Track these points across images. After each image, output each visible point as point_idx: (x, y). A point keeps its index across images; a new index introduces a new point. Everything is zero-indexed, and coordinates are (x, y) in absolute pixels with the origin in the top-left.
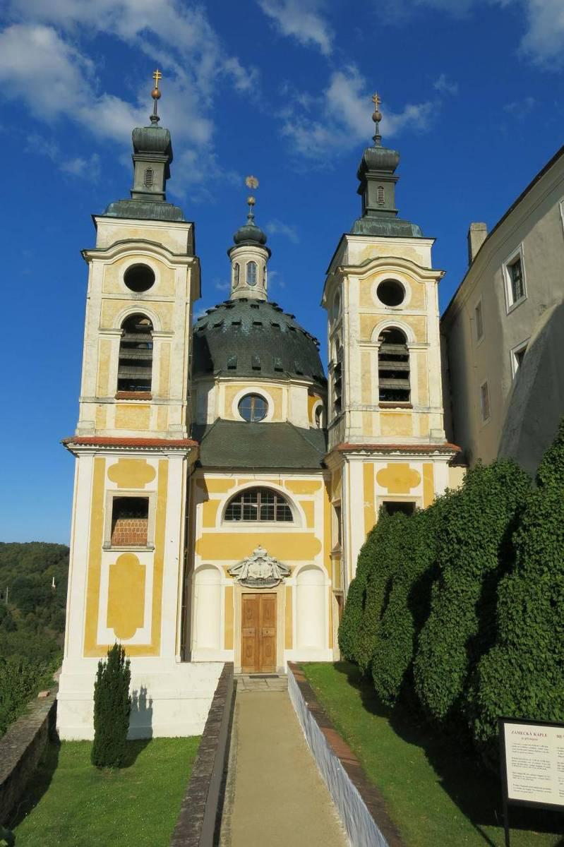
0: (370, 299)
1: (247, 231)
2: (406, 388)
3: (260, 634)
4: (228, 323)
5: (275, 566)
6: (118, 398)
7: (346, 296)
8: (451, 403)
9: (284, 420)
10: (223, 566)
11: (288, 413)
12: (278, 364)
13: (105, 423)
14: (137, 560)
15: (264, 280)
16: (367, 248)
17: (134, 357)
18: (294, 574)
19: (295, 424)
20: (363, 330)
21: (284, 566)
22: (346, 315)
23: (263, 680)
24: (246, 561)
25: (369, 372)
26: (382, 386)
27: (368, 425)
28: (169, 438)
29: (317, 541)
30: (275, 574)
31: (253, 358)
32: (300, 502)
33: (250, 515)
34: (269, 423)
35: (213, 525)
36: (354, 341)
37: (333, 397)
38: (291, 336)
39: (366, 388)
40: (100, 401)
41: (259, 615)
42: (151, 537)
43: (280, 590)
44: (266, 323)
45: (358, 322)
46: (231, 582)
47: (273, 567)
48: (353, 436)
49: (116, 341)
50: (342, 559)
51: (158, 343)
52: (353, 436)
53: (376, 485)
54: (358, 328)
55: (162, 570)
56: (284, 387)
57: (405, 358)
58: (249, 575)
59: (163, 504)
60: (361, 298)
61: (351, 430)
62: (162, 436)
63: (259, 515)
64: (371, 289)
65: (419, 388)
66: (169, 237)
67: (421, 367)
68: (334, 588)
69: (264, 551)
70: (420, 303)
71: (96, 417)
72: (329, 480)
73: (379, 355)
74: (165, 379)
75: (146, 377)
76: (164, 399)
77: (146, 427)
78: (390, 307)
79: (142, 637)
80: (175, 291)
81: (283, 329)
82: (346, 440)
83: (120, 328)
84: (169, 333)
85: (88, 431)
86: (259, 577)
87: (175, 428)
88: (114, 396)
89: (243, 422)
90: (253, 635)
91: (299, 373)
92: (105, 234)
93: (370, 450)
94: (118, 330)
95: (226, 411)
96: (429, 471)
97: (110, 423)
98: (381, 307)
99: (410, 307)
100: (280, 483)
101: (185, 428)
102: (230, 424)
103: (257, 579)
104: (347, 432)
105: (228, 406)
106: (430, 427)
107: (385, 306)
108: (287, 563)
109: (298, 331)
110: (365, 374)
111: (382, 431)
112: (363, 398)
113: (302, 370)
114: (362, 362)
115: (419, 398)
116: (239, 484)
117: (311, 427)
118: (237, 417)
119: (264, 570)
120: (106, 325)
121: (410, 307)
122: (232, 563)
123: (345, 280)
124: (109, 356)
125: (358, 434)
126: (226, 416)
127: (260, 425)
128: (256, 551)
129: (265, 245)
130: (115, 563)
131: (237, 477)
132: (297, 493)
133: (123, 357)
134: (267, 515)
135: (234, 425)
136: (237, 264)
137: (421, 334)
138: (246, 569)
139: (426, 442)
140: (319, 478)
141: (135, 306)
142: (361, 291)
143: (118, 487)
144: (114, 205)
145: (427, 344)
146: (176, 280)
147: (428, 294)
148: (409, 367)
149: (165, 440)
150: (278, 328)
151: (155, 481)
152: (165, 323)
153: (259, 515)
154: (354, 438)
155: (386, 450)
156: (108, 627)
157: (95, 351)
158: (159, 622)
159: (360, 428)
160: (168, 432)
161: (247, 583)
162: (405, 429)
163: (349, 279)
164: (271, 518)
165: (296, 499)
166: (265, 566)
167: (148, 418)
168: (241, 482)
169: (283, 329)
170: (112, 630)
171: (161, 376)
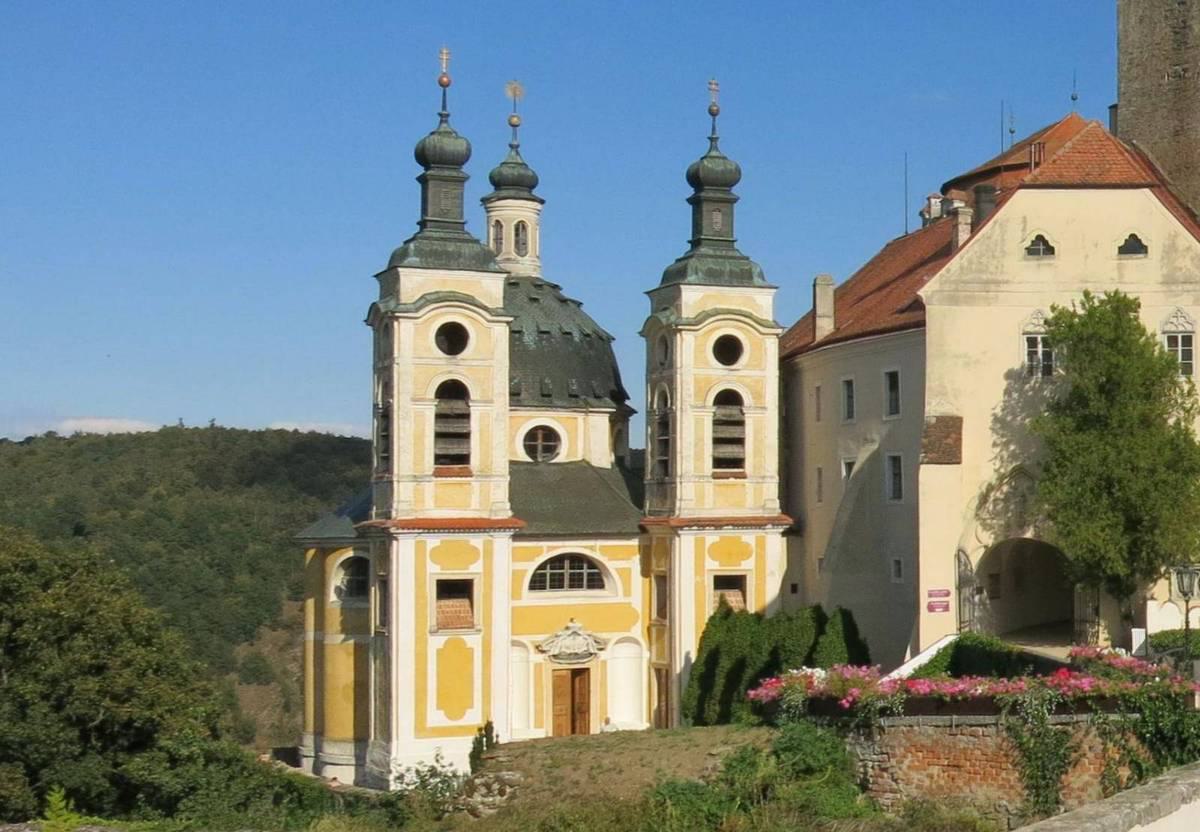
1: (513, 174)
2: (741, 456)
5: (590, 640)
9: (580, 459)
10: (532, 642)
11: (584, 449)
18: (610, 647)
19: (595, 463)
22: (678, 376)
25: (703, 440)
26: (716, 455)
27: (700, 497)
29: (635, 611)
31: (541, 382)
32: (617, 569)
33: (557, 583)
35: (520, 598)
36: (686, 406)
38: (586, 346)
39: (699, 457)
44: (555, 331)
45: (692, 389)
46: (540, 658)
48: (684, 509)
52: (684, 509)
56: (580, 417)
57: (741, 423)
58: (563, 650)
60: (696, 357)
61: (683, 503)
63: (566, 582)
68: (654, 660)
70: (758, 364)
72: (648, 543)
81: (577, 337)
82: (677, 512)
86: (572, 651)
89: (528, 463)
91: (597, 397)
93: (701, 524)
100: (592, 548)
103: (570, 654)
104: (678, 504)
107: (720, 365)
108: (603, 636)
109: (594, 336)
110: (699, 440)
111: (714, 503)
112: (695, 468)
116: (548, 551)
119: (578, 645)
121: (746, 367)
123: (678, 335)
125: (689, 507)
127: (553, 468)
128: (570, 625)
129: (536, 192)
131: (545, 544)
134: (576, 583)
135: (522, 468)
136: (498, 221)
137: (758, 396)
139: (759, 513)
140: (635, 542)
145: (764, 408)
148: (744, 432)
150: (569, 336)
153: (566, 582)
154: (686, 511)
155: (717, 524)
159: (691, 500)
163: (684, 336)
164: (581, 586)
165: (611, 565)
169: (577, 337)
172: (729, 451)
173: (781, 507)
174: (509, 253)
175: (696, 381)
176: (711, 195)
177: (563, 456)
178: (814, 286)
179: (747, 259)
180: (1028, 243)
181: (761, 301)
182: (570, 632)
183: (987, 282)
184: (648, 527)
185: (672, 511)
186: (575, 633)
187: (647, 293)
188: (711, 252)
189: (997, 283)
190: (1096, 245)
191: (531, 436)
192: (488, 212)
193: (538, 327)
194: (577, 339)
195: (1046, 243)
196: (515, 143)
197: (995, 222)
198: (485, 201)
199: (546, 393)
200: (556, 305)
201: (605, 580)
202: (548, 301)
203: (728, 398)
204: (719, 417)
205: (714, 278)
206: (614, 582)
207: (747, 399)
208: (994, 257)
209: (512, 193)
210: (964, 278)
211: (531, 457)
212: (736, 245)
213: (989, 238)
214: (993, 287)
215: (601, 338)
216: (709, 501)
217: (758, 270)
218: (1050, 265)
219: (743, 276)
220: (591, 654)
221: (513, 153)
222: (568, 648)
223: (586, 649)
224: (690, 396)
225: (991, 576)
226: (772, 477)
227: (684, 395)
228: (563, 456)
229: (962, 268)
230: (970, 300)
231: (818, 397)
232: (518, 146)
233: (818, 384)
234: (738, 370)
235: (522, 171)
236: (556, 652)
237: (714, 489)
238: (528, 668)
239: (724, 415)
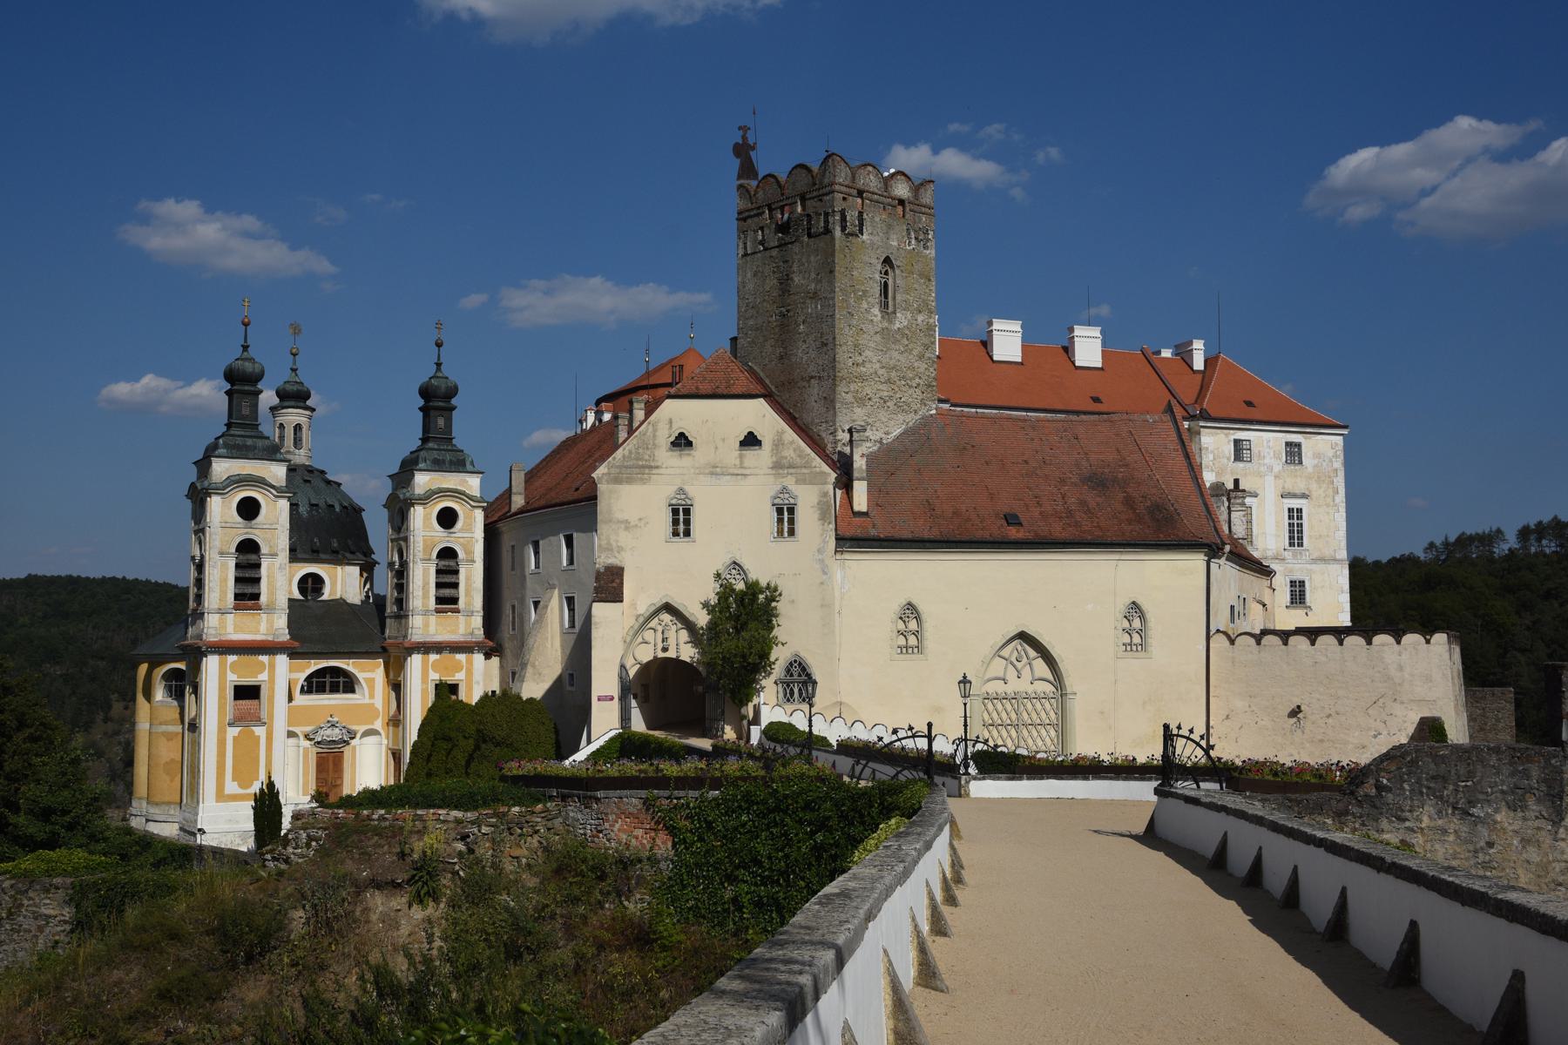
0: (431, 524)
7: (412, 521)
9: (338, 596)
14: (253, 732)
17: (247, 575)
18: (358, 736)
24: (321, 728)
25: (428, 584)
27: (426, 625)
31: (312, 541)
33: (321, 689)
37: (392, 595)
39: (425, 596)
40: (222, 612)
42: (264, 715)
43: (347, 750)
44: (322, 504)
45: (421, 544)
47: (344, 731)
49: (232, 563)
50: (401, 727)
51: (265, 564)
54: (421, 549)
56: (339, 568)
57: (456, 572)
58: (324, 738)
59: (272, 690)
60: (424, 523)
61: (414, 630)
62: (270, 638)
63: (328, 688)
65: (466, 596)
66: (271, 472)
67: (468, 578)
68: (390, 746)
69: (336, 719)
70: (469, 528)
74: (272, 592)
75: (256, 591)
76: (271, 609)
77: (257, 632)
81: (338, 509)
83: (234, 551)
84: (274, 555)
85: (215, 636)
87: (281, 631)
92: (219, 469)
96: (470, 663)
97: (230, 629)
101: (287, 631)
104: (410, 630)
106: (473, 626)
107: (442, 530)
108: (354, 727)
110: (426, 584)
112: (423, 603)
114: (423, 576)
115: (465, 604)
119: (335, 734)
120: (225, 549)
121: (461, 531)
122: (308, 729)
128: (330, 719)
129: (309, 403)
130: (236, 735)
133: (238, 575)
134: (335, 689)
136: (281, 425)
137: (469, 552)
141: (247, 533)
145: (474, 562)
146: (278, 510)
147: (477, 520)
149: (273, 641)
152: (271, 547)
153: (328, 688)
165: (360, 676)
167: (259, 623)
168: (315, 664)
169: (338, 509)
172: (447, 592)
173: (484, 634)
174: (289, 447)
175: (424, 540)
176: (436, 404)
177: (325, 597)
178: (511, 471)
179: (462, 451)
180: (672, 439)
181: (472, 484)
183: (643, 467)
184: (388, 648)
185: (405, 636)
186: (333, 725)
187: (389, 476)
188: (436, 447)
189: (651, 467)
190: (724, 440)
191: (303, 581)
192: (274, 417)
193: (309, 501)
194: (337, 510)
195: (686, 438)
196: (294, 367)
197: (649, 423)
198: (273, 409)
199: (315, 548)
200: (323, 485)
201: (356, 687)
202: (317, 482)
203: (448, 553)
204: (440, 567)
205: (438, 466)
206: (363, 688)
207: (461, 555)
208: (647, 448)
209: (292, 403)
210: (626, 464)
212: (454, 441)
213: (644, 434)
214: (647, 471)
215: (355, 509)
216: (432, 629)
217: (470, 459)
218: (689, 455)
219: (459, 464)
220: (345, 741)
221: (293, 374)
222: (328, 737)
225: (642, 685)
226: (478, 612)
227: (416, 551)
228: (325, 597)
229: (624, 456)
230: (630, 481)
231: (513, 552)
232: (297, 370)
233: (513, 543)
235: (300, 388)
236: (320, 739)
238: (299, 751)
239: (444, 566)
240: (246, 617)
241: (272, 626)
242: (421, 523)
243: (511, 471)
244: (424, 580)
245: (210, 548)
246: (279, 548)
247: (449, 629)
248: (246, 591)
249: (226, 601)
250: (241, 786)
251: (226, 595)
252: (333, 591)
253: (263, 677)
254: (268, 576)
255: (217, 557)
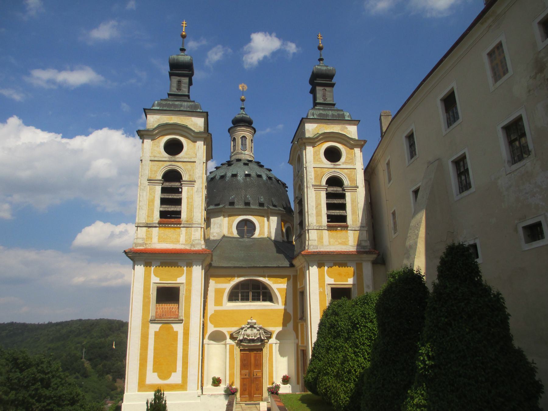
0: (320, 158)
3: (252, 375)
4: (229, 174)
6: (159, 223)
8: (373, 224)
10: (227, 331)
12: (261, 200)
13: (152, 239)
14: (172, 328)
15: (252, 147)
16: (317, 127)
17: (170, 197)
18: (274, 336)
20: (315, 178)
21: (267, 330)
23: (254, 406)
25: (320, 204)
26: (329, 213)
27: (320, 238)
28: (193, 249)
30: (262, 336)
32: (278, 289)
33: (245, 298)
34: (257, 238)
35: (221, 305)
36: (310, 185)
39: (319, 214)
41: (251, 363)
44: (253, 174)
45: (313, 174)
53: (326, 277)
55: (188, 334)
58: (245, 337)
59: (189, 291)
60: (314, 158)
62: (188, 247)
64: (320, 152)
66: (192, 121)
69: (254, 321)
71: (146, 236)
73: (327, 194)
74: (190, 210)
75: (178, 209)
78: (333, 163)
79: (176, 378)
80: (196, 155)
81: (264, 178)
82: (307, 248)
83: (160, 178)
85: (141, 245)
86: (251, 338)
87: (197, 242)
88: (157, 222)
89: (238, 238)
90: (247, 376)
94: (160, 181)
95: (228, 231)
97: (155, 239)
98: (327, 163)
99: (345, 163)
102: (230, 239)
105: (230, 227)
107: (329, 163)
108: (270, 329)
109: (274, 179)
110: (318, 205)
111: (329, 242)
112: (317, 221)
113: (277, 204)
114: (316, 198)
117: (283, 240)
118: (235, 233)
121: (343, 163)
122: (234, 329)
124: (154, 197)
126: (228, 233)
128: (249, 321)
132: (275, 283)
133: (163, 197)
134: (256, 298)
135: (234, 240)
137: (353, 180)
138: (243, 333)
142: (314, 153)
143: (160, 281)
144: (158, 102)
151: (184, 276)
152: (190, 175)
156: (153, 372)
157: (145, 194)
158: (187, 368)
159: (315, 240)
160: (192, 245)
161: (244, 342)
162: (344, 240)
166: (255, 331)
167: (180, 236)
169: (264, 178)
170: (156, 374)
171: (187, 208)
174: (238, 150)
182: (249, 326)
199: (247, 201)
203: (335, 181)
207: (346, 182)
211: (239, 235)
222: (248, 336)
223: (259, 336)
224: (311, 179)
228: (257, 235)
234: (340, 165)
236: (241, 338)
237: (329, 234)
240: (169, 232)
241: (190, 238)
242: (312, 158)
243: (380, 119)
244: (316, 201)
245: (141, 176)
246: (197, 176)
247: (340, 241)
248: (169, 209)
249: (153, 217)
250: (161, 377)
251: (153, 212)
252: (261, 232)
253: (182, 279)
254: (188, 198)
255: (146, 183)
